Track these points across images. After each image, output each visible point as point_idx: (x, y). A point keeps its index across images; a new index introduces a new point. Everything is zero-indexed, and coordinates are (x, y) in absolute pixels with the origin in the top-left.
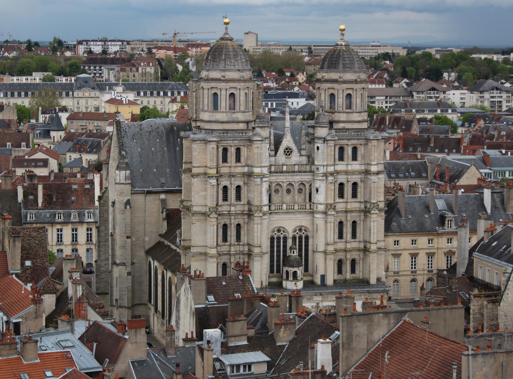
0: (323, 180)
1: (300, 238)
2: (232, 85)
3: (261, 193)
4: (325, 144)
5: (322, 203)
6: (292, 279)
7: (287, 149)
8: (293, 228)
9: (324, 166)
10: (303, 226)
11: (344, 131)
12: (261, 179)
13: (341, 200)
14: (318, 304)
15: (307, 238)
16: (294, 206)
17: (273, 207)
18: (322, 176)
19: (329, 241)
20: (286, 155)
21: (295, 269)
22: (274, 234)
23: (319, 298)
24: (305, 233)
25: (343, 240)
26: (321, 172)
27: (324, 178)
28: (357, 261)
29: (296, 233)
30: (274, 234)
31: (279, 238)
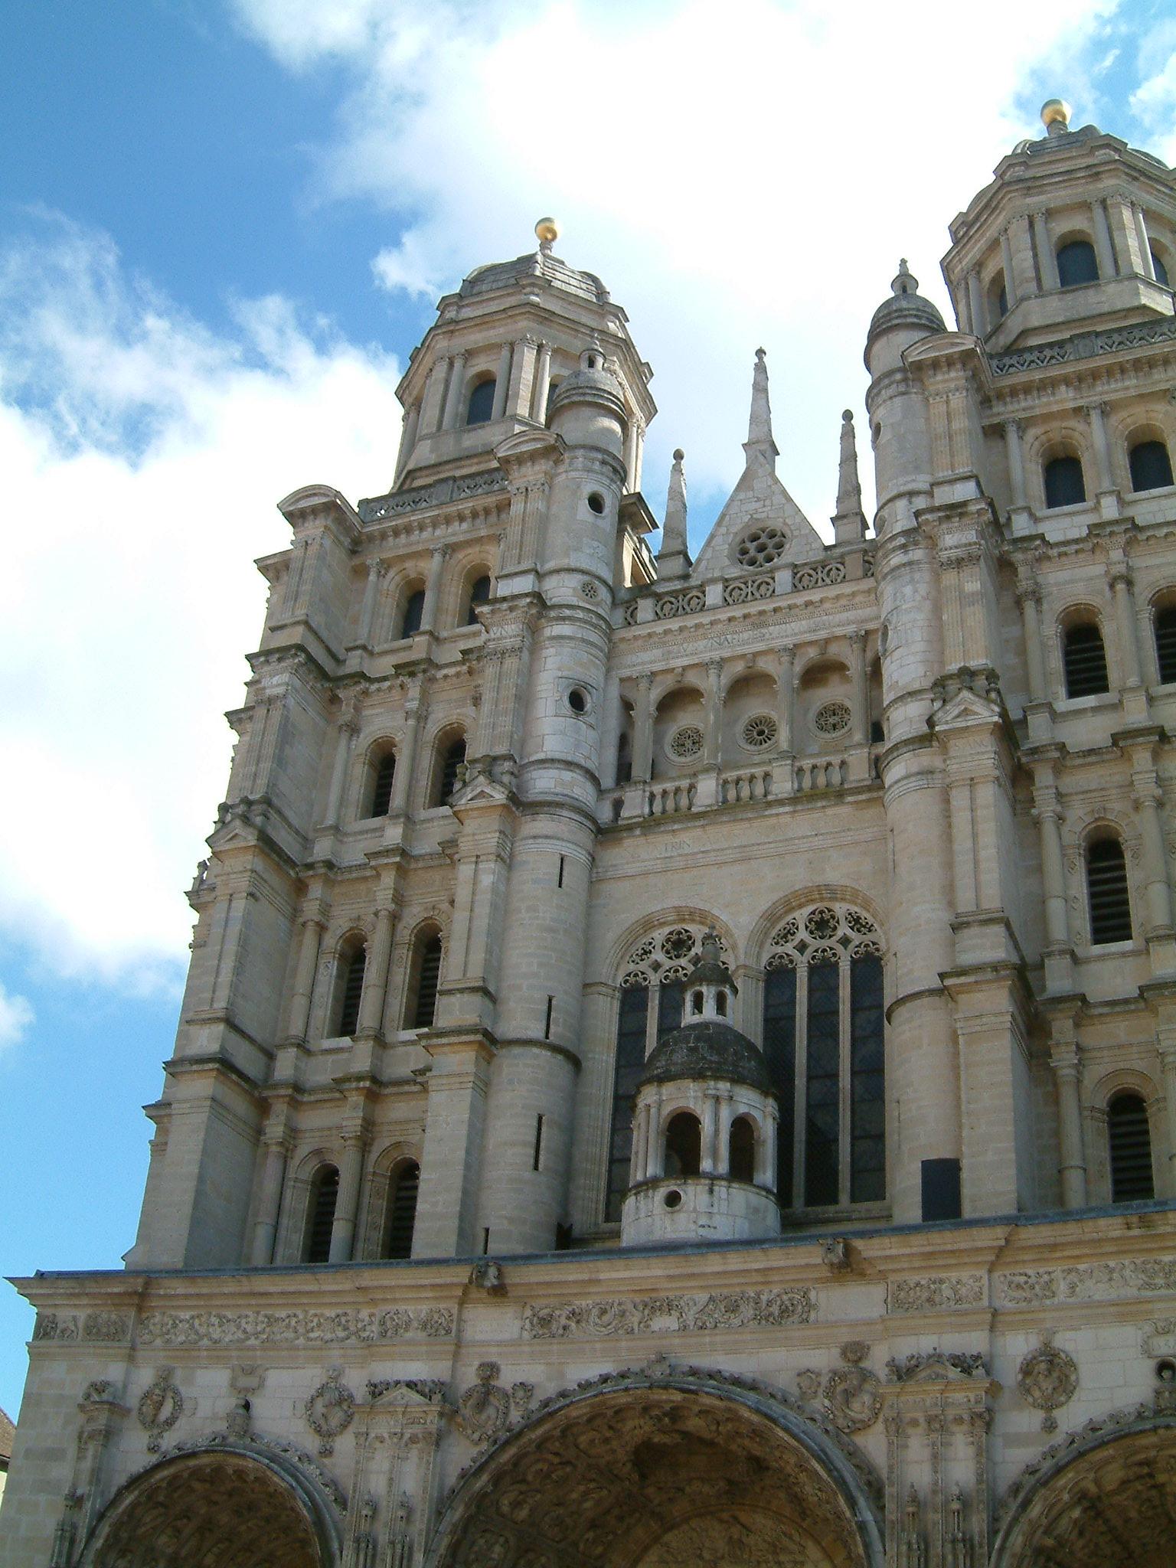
0: (910, 563)
1: (823, 971)
2: (475, 338)
3: (524, 699)
4: (915, 399)
5: (916, 686)
6: (654, 1168)
7: (754, 538)
8: (764, 904)
9: (911, 494)
10: (832, 892)
11: (1048, 353)
12: (533, 629)
13: (1090, 701)
14: (855, 1352)
15: (869, 968)
16: (767, 776)
17: (635, 803)
18: (903, 547)
19: (965, 901)
20: (752, 562)
21: (687, 1095)
22: (643, 966)
23: (855, 1304)
24: (856, 938)
25: (1127, 945)
26: (898, 529)
27: (917, 554)
29: (789, 948)
30: (643, 966)
31: (673, 991)
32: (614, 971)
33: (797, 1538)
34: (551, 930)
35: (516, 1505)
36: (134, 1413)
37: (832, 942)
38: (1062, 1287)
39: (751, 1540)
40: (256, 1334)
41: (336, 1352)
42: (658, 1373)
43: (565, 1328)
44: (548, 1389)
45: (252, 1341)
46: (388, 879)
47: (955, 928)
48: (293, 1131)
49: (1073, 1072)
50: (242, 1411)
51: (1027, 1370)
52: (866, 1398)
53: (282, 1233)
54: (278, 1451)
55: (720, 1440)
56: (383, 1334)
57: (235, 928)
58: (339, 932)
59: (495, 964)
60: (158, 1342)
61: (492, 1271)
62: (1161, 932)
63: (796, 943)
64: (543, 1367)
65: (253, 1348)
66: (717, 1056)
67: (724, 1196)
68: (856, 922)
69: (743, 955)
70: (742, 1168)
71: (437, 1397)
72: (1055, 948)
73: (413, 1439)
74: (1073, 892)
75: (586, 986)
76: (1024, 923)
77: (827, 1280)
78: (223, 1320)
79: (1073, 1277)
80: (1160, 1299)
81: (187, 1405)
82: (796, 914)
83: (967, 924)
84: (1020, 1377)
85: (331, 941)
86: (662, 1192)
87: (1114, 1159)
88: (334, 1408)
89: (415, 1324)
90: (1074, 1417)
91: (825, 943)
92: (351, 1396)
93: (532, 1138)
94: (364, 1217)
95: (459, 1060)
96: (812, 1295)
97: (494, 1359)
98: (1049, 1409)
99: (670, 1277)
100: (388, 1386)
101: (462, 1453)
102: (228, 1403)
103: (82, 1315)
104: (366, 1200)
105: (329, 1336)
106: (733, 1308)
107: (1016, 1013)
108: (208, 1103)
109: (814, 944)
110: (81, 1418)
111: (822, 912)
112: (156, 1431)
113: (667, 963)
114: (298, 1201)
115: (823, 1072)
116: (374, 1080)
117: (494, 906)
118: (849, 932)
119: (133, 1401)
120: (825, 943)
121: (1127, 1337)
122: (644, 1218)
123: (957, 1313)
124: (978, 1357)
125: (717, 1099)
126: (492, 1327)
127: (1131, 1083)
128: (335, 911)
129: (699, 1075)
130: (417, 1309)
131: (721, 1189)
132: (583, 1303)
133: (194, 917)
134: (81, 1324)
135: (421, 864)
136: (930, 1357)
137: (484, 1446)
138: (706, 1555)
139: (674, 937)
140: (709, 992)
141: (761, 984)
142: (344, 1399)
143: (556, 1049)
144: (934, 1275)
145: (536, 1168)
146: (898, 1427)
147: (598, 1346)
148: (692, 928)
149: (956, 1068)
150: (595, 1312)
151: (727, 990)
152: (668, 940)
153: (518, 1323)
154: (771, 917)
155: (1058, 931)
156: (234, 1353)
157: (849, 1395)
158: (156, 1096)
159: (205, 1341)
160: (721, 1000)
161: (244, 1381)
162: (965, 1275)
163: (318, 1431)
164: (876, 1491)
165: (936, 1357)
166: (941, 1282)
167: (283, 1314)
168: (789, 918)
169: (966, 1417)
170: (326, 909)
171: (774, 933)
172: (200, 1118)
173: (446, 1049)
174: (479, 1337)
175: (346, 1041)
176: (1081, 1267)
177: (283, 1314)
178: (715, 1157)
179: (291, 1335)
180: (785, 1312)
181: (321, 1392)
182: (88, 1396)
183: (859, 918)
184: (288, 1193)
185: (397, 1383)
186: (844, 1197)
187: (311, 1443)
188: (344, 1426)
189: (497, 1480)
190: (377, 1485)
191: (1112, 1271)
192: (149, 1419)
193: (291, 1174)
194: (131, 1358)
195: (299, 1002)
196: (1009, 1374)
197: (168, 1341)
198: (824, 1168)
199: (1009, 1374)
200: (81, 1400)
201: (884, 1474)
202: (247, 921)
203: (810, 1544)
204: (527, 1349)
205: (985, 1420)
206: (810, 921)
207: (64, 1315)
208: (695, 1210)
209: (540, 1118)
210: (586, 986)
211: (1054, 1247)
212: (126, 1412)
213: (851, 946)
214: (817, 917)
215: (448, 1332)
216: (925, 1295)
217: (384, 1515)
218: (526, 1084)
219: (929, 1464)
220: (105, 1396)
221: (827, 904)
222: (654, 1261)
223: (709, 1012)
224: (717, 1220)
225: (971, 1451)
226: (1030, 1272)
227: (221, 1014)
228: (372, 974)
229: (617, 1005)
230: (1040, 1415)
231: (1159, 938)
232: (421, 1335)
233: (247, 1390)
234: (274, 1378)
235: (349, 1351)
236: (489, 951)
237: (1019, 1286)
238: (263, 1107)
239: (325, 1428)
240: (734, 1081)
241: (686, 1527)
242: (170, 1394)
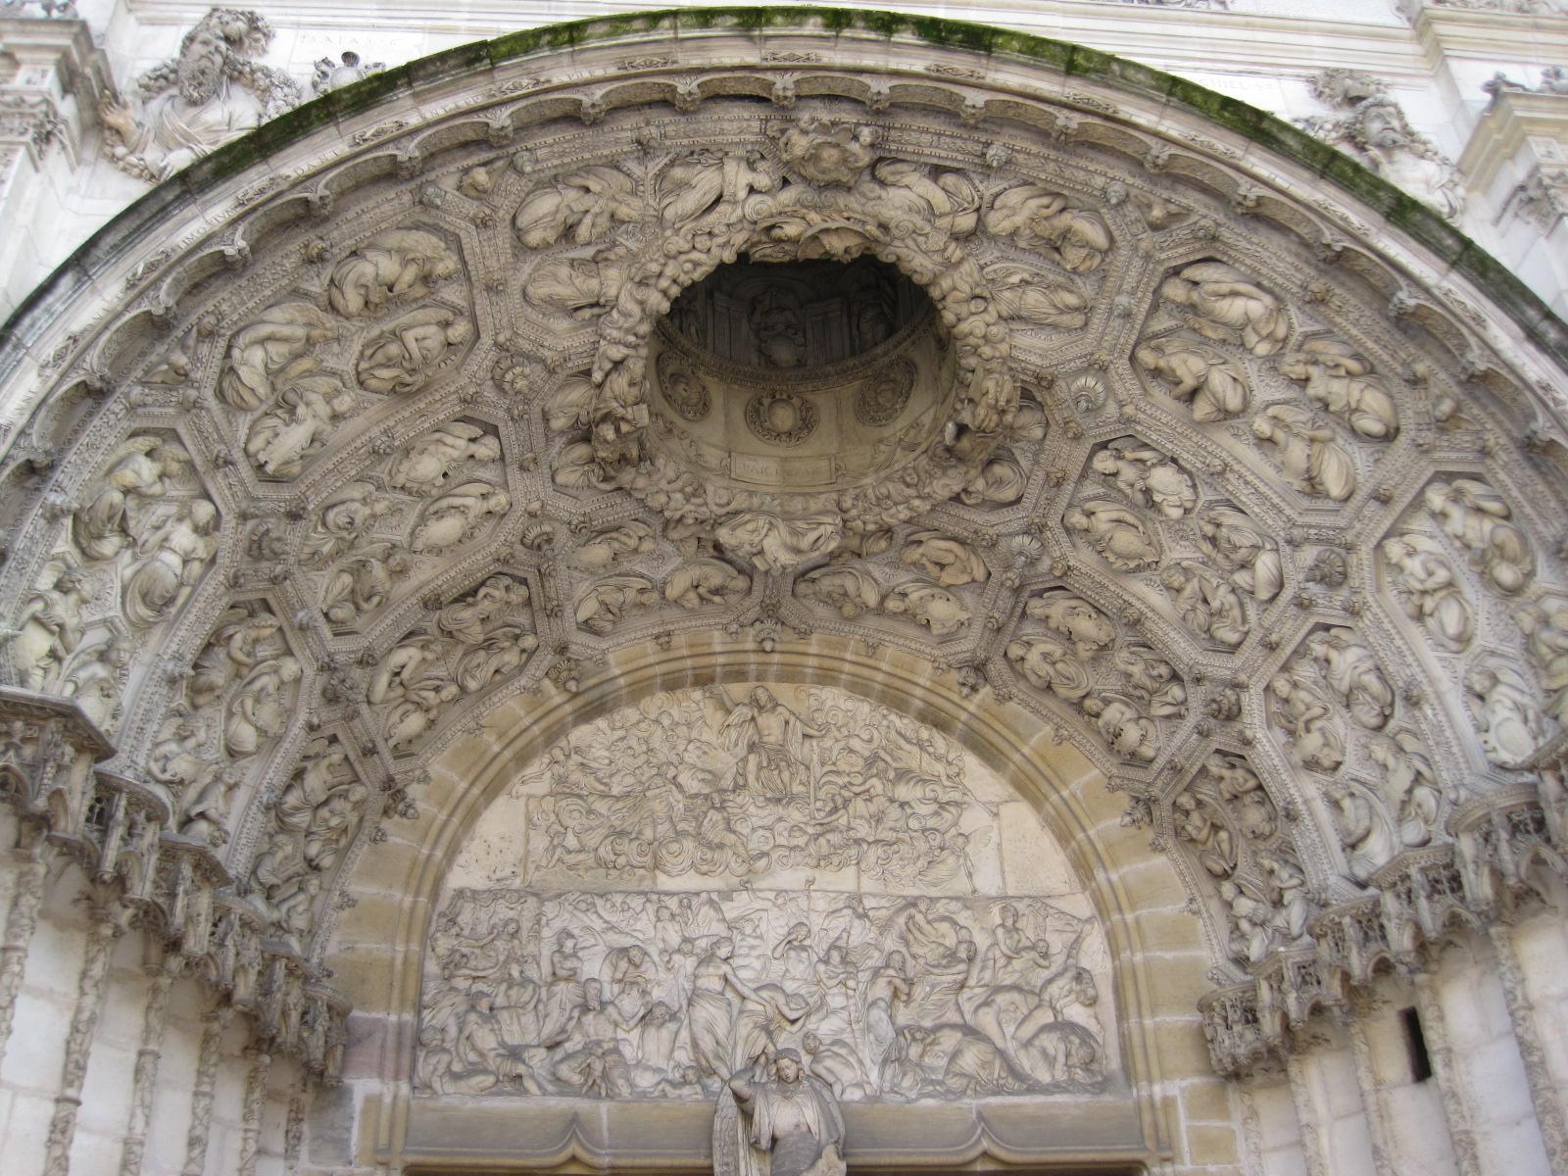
138: (691, 783)
241: (631, 714)
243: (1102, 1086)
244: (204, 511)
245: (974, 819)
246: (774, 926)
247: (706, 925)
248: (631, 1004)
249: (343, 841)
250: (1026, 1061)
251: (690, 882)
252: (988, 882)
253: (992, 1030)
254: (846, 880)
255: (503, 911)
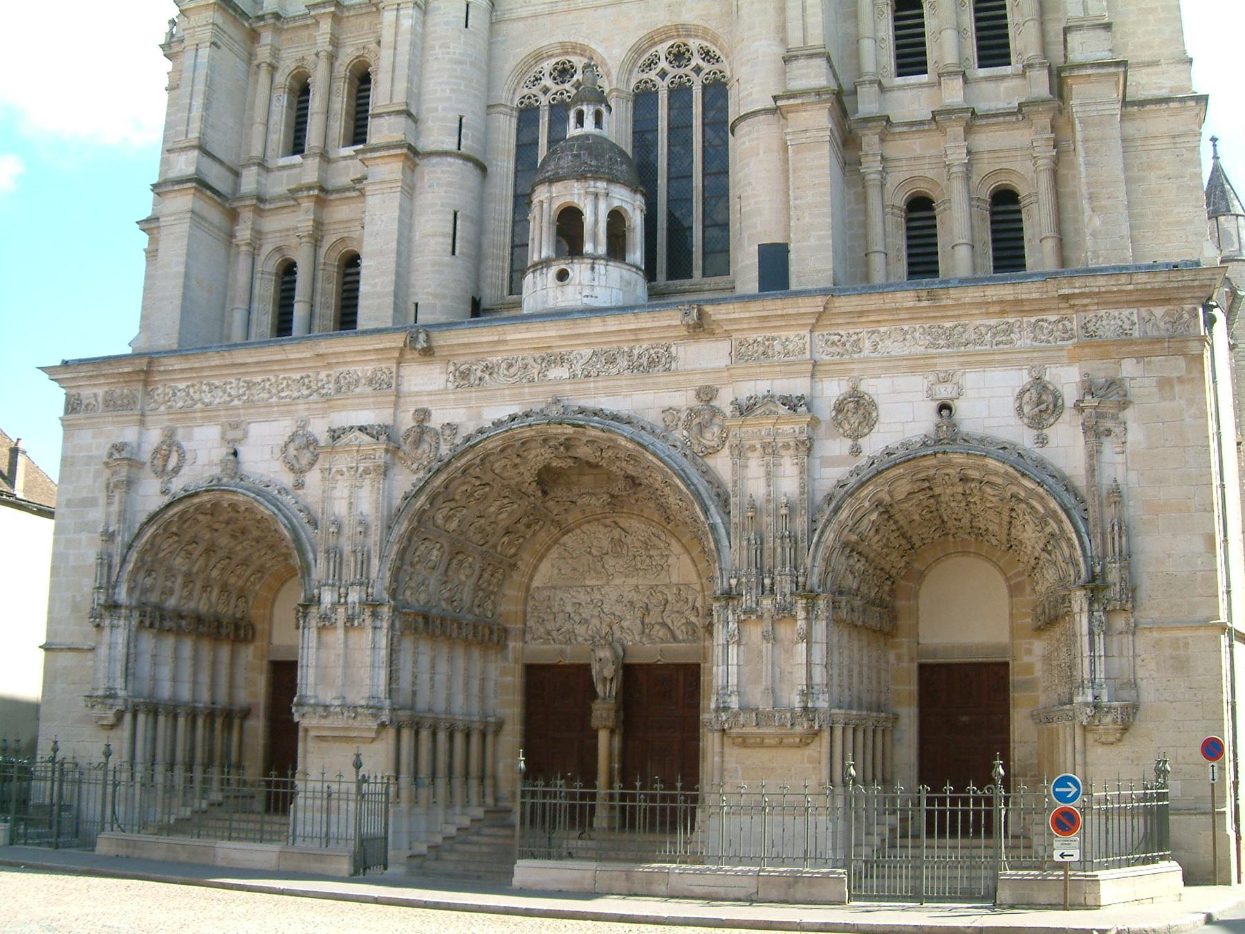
1: (680, 93)
6: (547, 251)
8: (632, 40)
10: (688, 31)
14: (707, 394)
15: (717, 91)
19: (795, 40)
21: (572, 193)
22: (535, 90)
23: (706, 356)
25: (923, 78)
28: (1023, 191)
29: (652, 75)
30: (535, 90)
31: (559, 111)
32: (511, 95)
33: (663, 537)
34: (460, 63)
35: (448, 518)
36: (148, 465)
37: (688, 70)
38: (867, 344)
39: (628, 540)
40: (239, 397)
41: (302, 407)
42: (554, 412)
43: (480, 379)
44: (470, 428)
45: (236, 402)
46: (326, 26)
47: (787, 60)
48: (258, 235)
49: (877, 177)
50: (232, 458)
51: (839, 408)
52: (716, 429)
53: (254, 316)
54: (261, 486)
55: (603, 463)
56: (339, 390)
57: (202, 73)
58: (287, 71)
59: (415, 91)
60: (163, 408)
61: (422, 337)
62: (950, 69)
63: (658, 70)
64: (464, 411)
65: (236, 408)
66: (595, 161)
67: (603, 272)
68: (706, 55)
69: (616, 79)
70: (616, 249)
71: (383, 438)
72: (866, 78)
73: (366, 471)
74: (881, 34)
75: (489, 107)
76: (841, 56)
77: (682, 338)
78: (212, 387)
79: (875, 337)
80: (941, 356)
81: (189, 456)
82: (658, 48)
83: (796, 57)
84: (834, 413)
85: (282, 78)
86: (554, 270)
87: (909, 247)
88: (304, 450)
89: (363, 381)
90: (875, 444)
91: (682, 71)
92: (316, 441)
93: (451, 232)
94: (318, 298)
95: (389, 170)
96: (673, 349)
97: (425, 406)
98: (856, 438)
99: (562, 337)
100: (344, 431)
101: (404, 480)
102: (222, 452)
103: (100, 392)
104: (319, 285)
105: (296, 394)
106: (611, 361)
107: (834, 129)
108: (189, 215)
109: (673, 72)
110: (107, 473)
111: (679, 46)
112: (166, 478)
113: (554, 88)
114: (266, 290)
115: (680, 175)
116: (322, 189)
117: (413, 44)
118: (701, 63)
119: (146, 456)
120: (682, 71)
121: (918, 383)
122: (539, 290)
123: (787, 364)
124: (801, 398)
125: (596, 195)
126: (424, 381)
127: (924, 188)
128: (284, 54)
129: (582, 177)
130: (364, 370)
131: (600, 266)
132: (494, 359)
133: (168, 65)
134: (100, 399)
135: (352, 13)
136: (765, 397)
137: (421, 474)
138: (594, 552)
139: (560, 67)
140: (589, 111)
141: (630, 104)
142: (310, 443)
143: (467, 158)
144: (768, 335)
145: (453, 253)
146: (740, 452)
147: (507, 392)
148: (572, 58)
149: (786, 172)
150: (504, 365)
151: (603, 109)
152: (555, 69)
153: (444, 377)
154: (638, 50)
155: (869, 66)
156: (222, 413)
157: (702, 427)
158: (147, 213)
159: (199, 405)
160: (598, 117)
161: (231, 434)
162: (791, 334)
163: (292, 469)
164: (724, 501)
165: (769, 398)
166: (774, 339)
167: (259, 379)
168: (652, 51)
169: (792, 444)
170: (275, 52)
171: (640, 63)
172: (184, 227)
173: (379, 161)
174: (413, 389)
175: (297, 159)
176: (882, 330)
177: (259, 379)
178: (595, 239)
179: (266, 395)
180: (652, 363)
181: (292, 439)
182: (111, 455)
183: (709, 51)
184: (257, 283)
185: (352, 428)
186: (697, 273)
187: (288, 479)
188: (312, 464)
189: (432, 500)
190: (340, 508)
191: (906, 333)
192: (159, 469)
193: (258, 268)
194: (142, 423)
195: (258, 129)
196: (825, 411)
197: (170, 407)
198: (680, 251)
199: (825, 411)
200: (105, 459)
201: (730, 488)
202: (212, 67)
203: (673, 541)
204: (452, 396)
205: (807, 446)
206: (670, 53)
207: (86, 393)
208: (580, 283)
209: (455, 214)
210: (489, 107)
211: (861, 313)
212: (141, 465)
213: (702, 74)
214: (675, 50)
215: (389, 386)
216: (761, 349)
217: (347, 531)
218: (443, 186)
219: (765, 480)
220: (124, 454)
221: (684, 40)
222: (548, 324)
223: (589, 126)
224: (597, 291)
225: (796, 470)
226: (842, 333)
227: (195, 143)
228: (316, 103)
229: (514, 122)
230: (849, 442)
231: (949, 74)
232: (369, 389)
233: (234, 441)
234: (256, 430)
235: (315, 406)
236: (410, 81)
237: (833, 343)
238: (233, 216)
239: (297, 466)
240: (610, 181)
241: (578, 531)
242: (175, 448)
243: (694, 641)
244: (438, 546)
245: (672, 560)
246: (614, 596)
247: (597, 596)
248: (577, 618)
249: (500, 585)
250: (678, 633)
251: (594, 582)
252: (674, 579)
253: (670, 624)
254: (634, 581)
255: (546, 593)
